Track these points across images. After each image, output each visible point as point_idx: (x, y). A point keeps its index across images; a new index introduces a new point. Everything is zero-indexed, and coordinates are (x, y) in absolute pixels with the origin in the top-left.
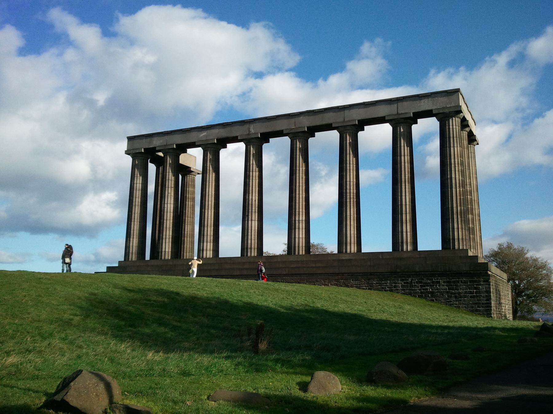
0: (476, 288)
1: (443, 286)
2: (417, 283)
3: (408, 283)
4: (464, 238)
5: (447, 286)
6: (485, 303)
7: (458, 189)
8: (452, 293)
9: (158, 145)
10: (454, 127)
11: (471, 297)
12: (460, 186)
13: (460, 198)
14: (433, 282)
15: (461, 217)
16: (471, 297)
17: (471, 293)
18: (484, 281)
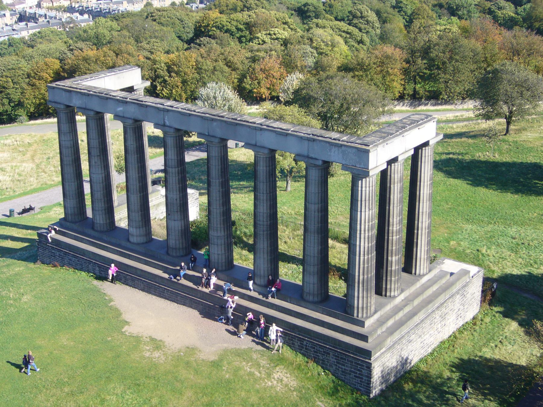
0: (359, 370)
1: (333, 358)
2: (311, 347)
3: (303, 344)
4: (365, 306)
5: (336, 359)
6: (366, 386)
7: (362, 258)
8: (339, 367)
9: (77, 106)
10: (364, 189)
11: (355, 376)
12: (364, 254)
13: (364, 267)
14: (324, 352)
15: (363, 286)
16: (355, 376)
17: (354, 373)
18: (366, 367)
